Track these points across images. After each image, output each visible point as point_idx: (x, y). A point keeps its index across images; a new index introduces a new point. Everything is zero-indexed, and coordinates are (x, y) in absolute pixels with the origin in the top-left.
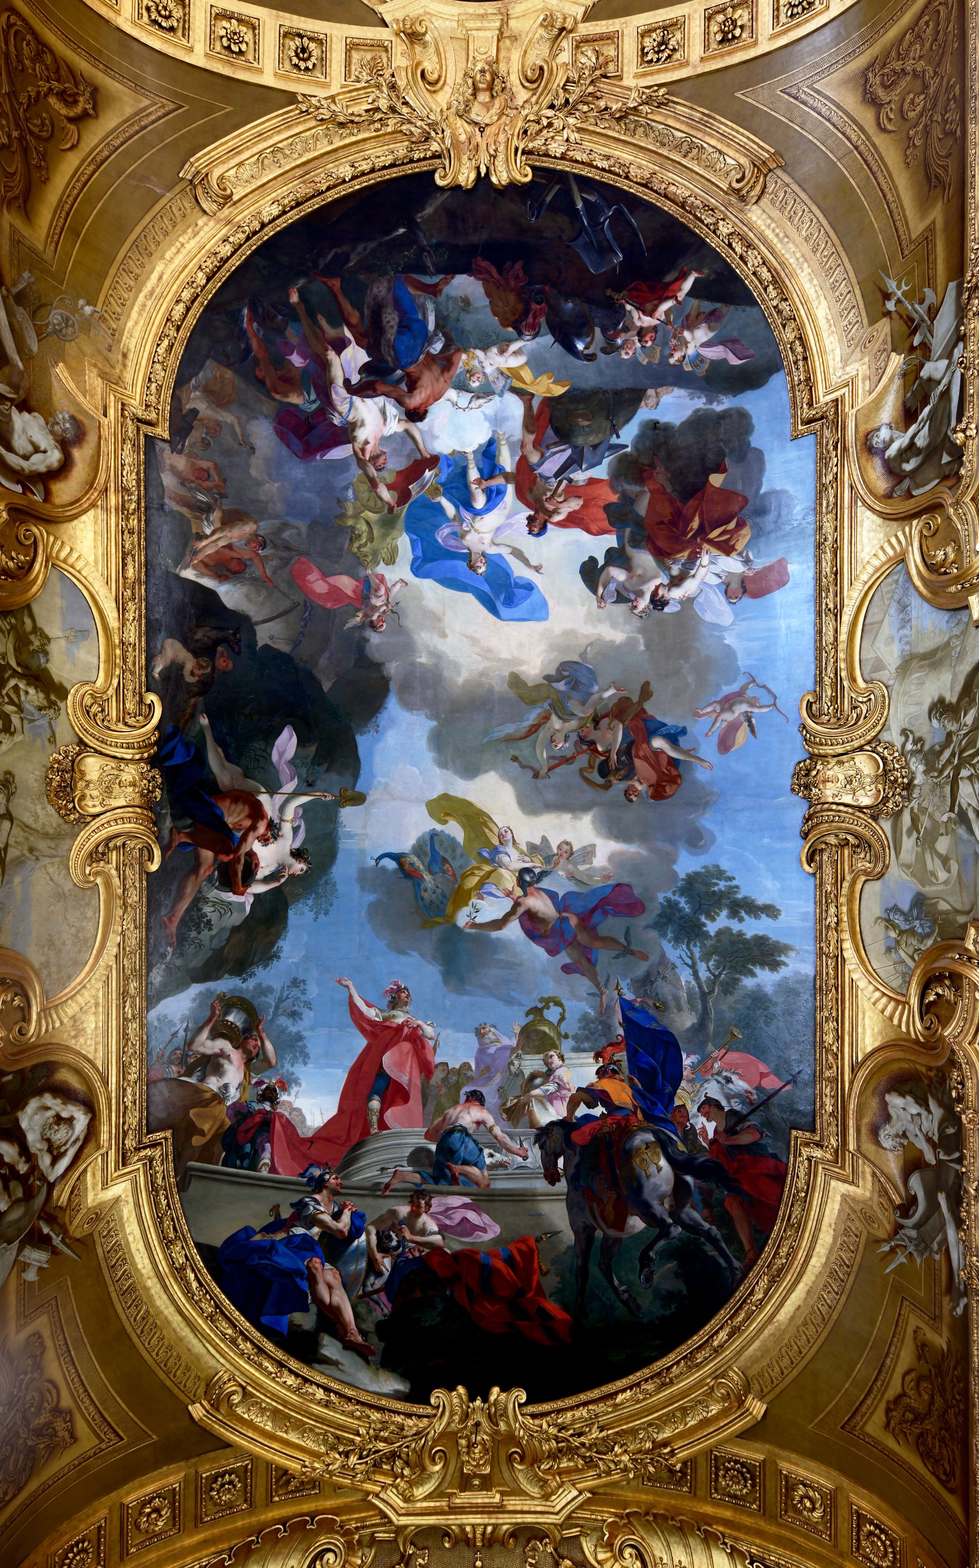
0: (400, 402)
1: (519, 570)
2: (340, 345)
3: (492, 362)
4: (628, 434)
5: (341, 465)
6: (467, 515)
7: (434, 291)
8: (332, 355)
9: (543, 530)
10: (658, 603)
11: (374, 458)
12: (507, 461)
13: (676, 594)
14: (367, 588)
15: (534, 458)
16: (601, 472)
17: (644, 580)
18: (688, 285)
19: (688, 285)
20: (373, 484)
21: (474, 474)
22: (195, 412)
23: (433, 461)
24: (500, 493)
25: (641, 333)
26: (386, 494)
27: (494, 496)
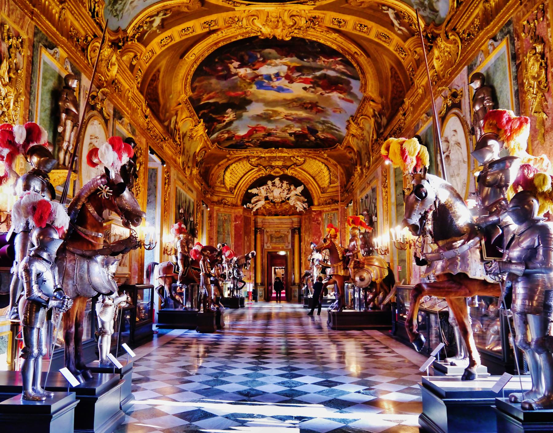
0: (250, 68)
1: (285, 87)
2: (231, 63)
3: (278, 61)
4: (318, 74)
5: (236, 79)
6: (271, 82)
7: (259, 52)
8: (230, 65)
9: (293, 83)
10: (321, 94)
11: (244, 77)
12: (282, 74)
13: (327, 95)
14: (245, 93)
15: (291, 74)
16: (310, 77)
17: (319, 91)
18: (340, 59)
19: (340, 59)
20: (244, 80)
21: (273, 77)
22: (196, 86)
23: (261, 75)
24: (280, 79)
25: (324, 61)
26: (248, 81)
27: (278, 80)
